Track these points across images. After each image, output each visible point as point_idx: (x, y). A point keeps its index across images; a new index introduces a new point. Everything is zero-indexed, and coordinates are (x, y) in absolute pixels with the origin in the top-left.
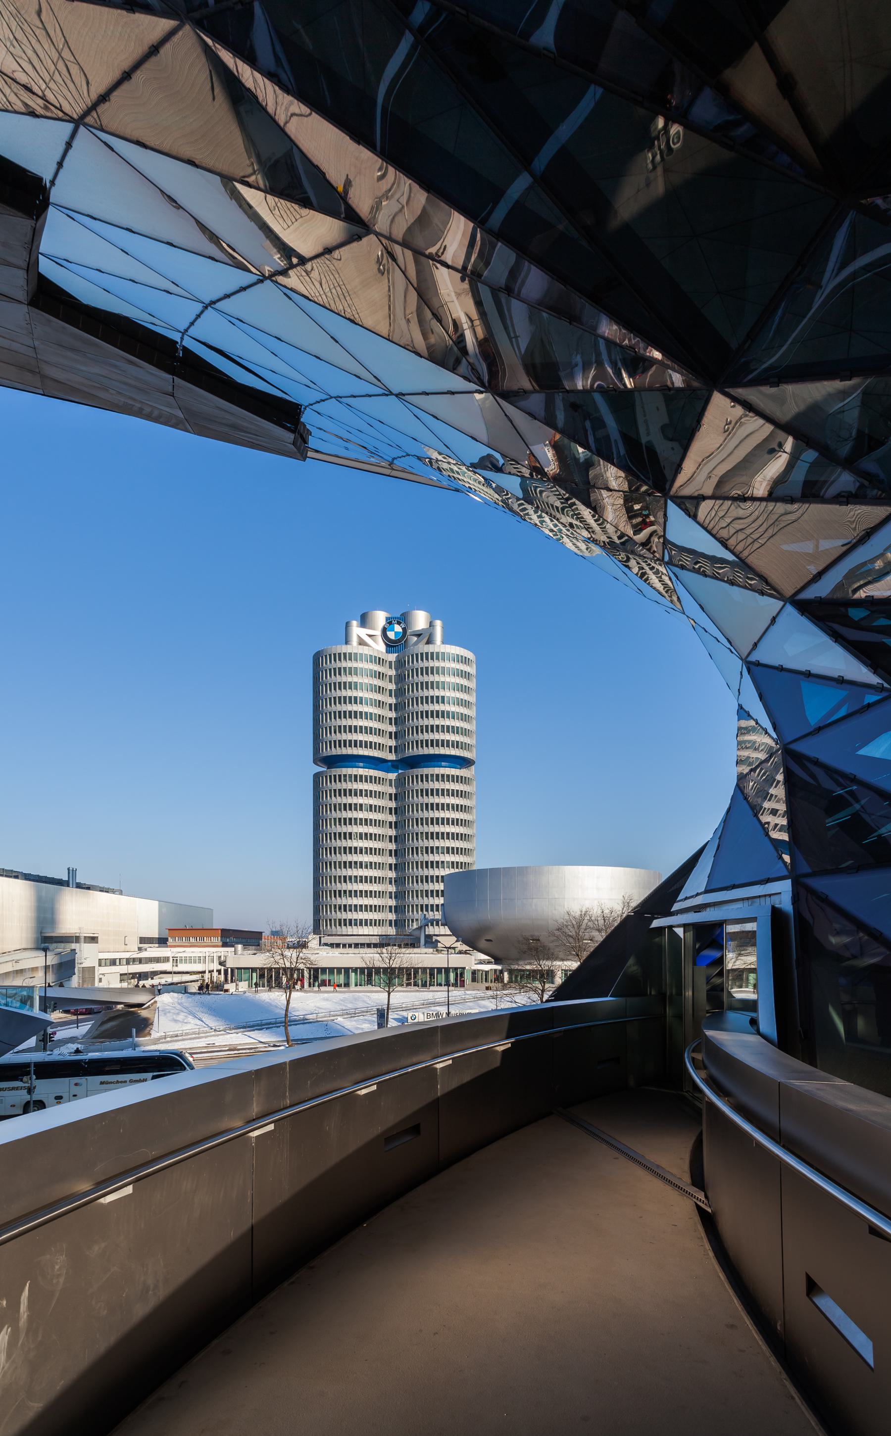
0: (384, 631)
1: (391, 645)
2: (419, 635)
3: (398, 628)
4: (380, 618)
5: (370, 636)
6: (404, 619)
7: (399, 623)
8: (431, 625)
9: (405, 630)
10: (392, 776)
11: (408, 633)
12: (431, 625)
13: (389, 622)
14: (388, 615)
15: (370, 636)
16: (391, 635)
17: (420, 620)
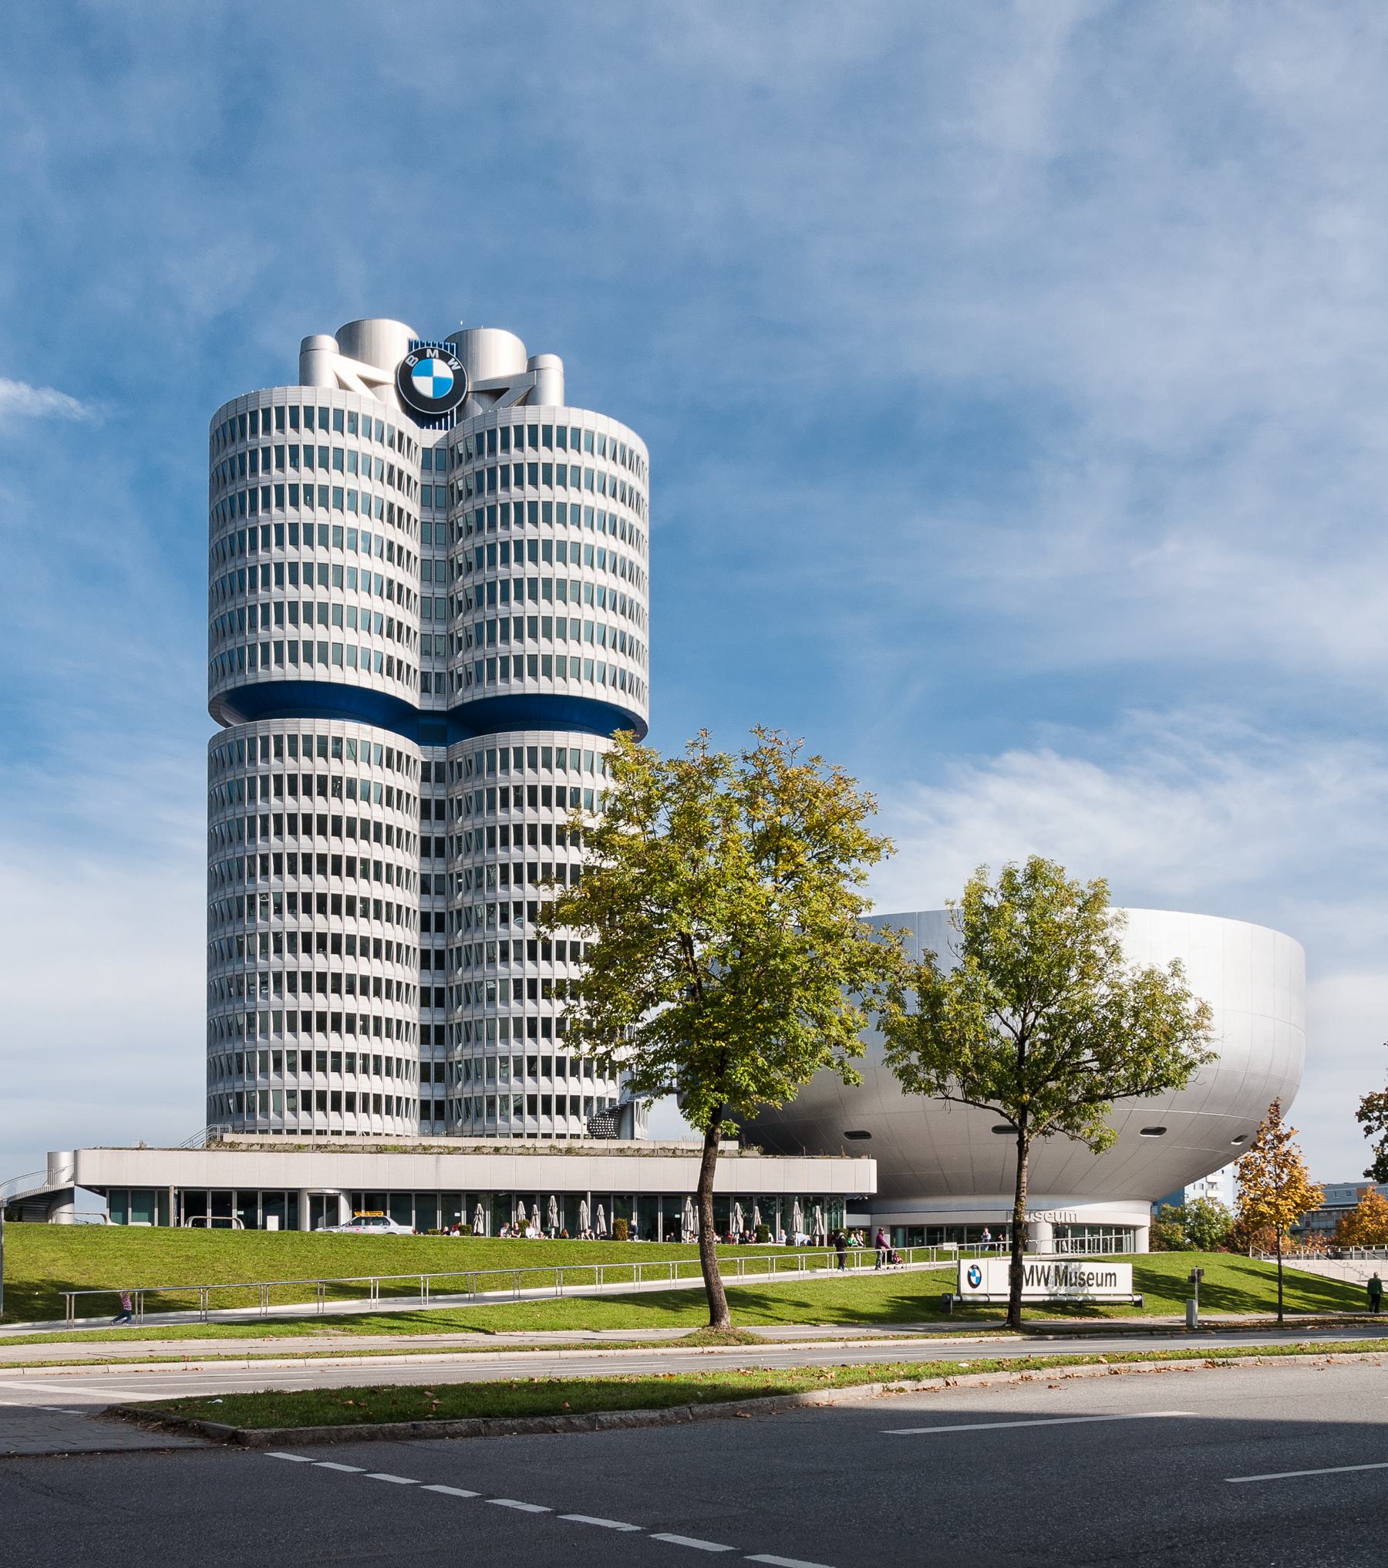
0: (405, 375)
1: (420, 410)
2: (495, 393)
3: (443, 370)
4: (393, 339)
5: (371, 384)
6: (458, 347)
7: (445, 357)
8: (533, 365)
9: (459, 376)
10: (439, 753)
11: (469, 386)
12: (533, 365)
13: (418, 351)
14: (414, 337)
15: (371, 384)
16: (424, 385)
17: (501, 355)
